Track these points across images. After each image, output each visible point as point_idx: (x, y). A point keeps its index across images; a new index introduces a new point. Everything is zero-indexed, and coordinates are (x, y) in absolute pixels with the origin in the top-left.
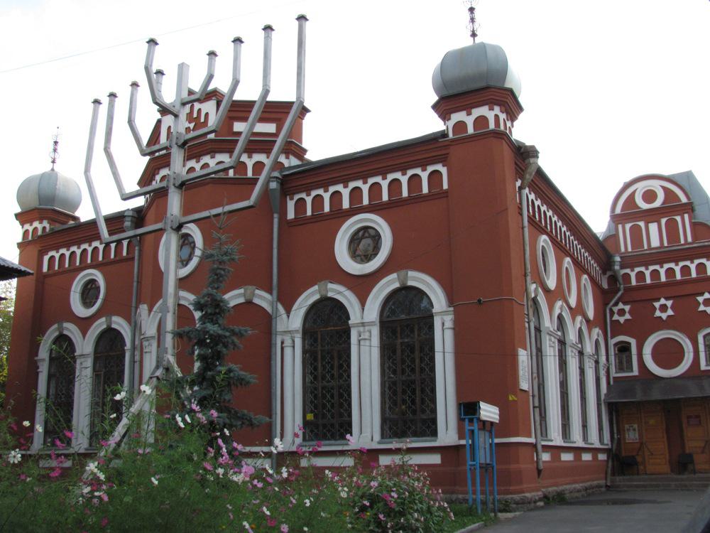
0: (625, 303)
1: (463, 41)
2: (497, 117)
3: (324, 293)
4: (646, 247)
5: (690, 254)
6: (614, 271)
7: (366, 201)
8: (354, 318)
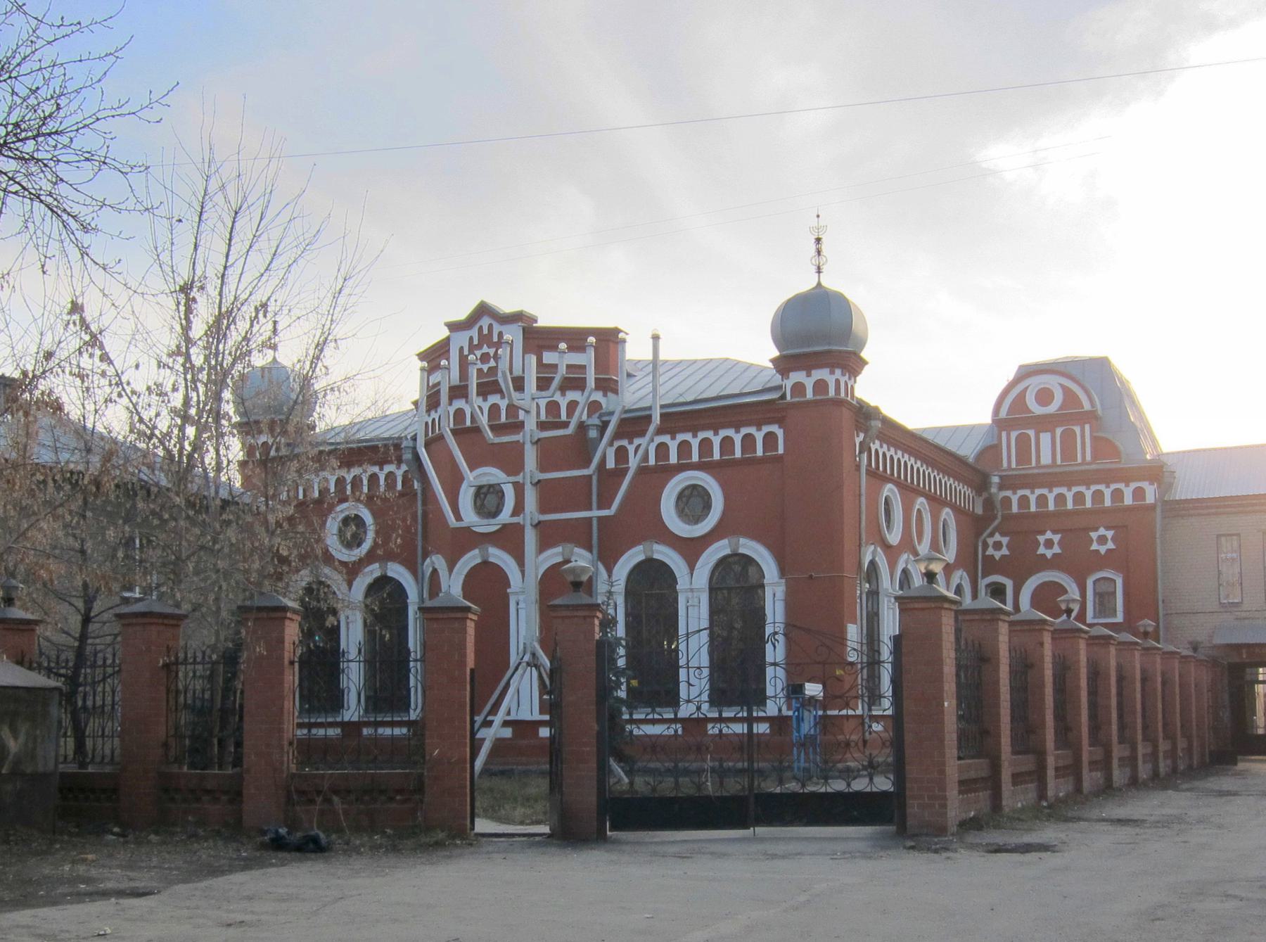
0: (1003, 534)
1: (805, 283)
2: (837, 381)
3: (649, 554)
4: (1034, 464)
5: (1087, 479)
6: (990, 494)
7: (695, 457)
8: (682, 584)
